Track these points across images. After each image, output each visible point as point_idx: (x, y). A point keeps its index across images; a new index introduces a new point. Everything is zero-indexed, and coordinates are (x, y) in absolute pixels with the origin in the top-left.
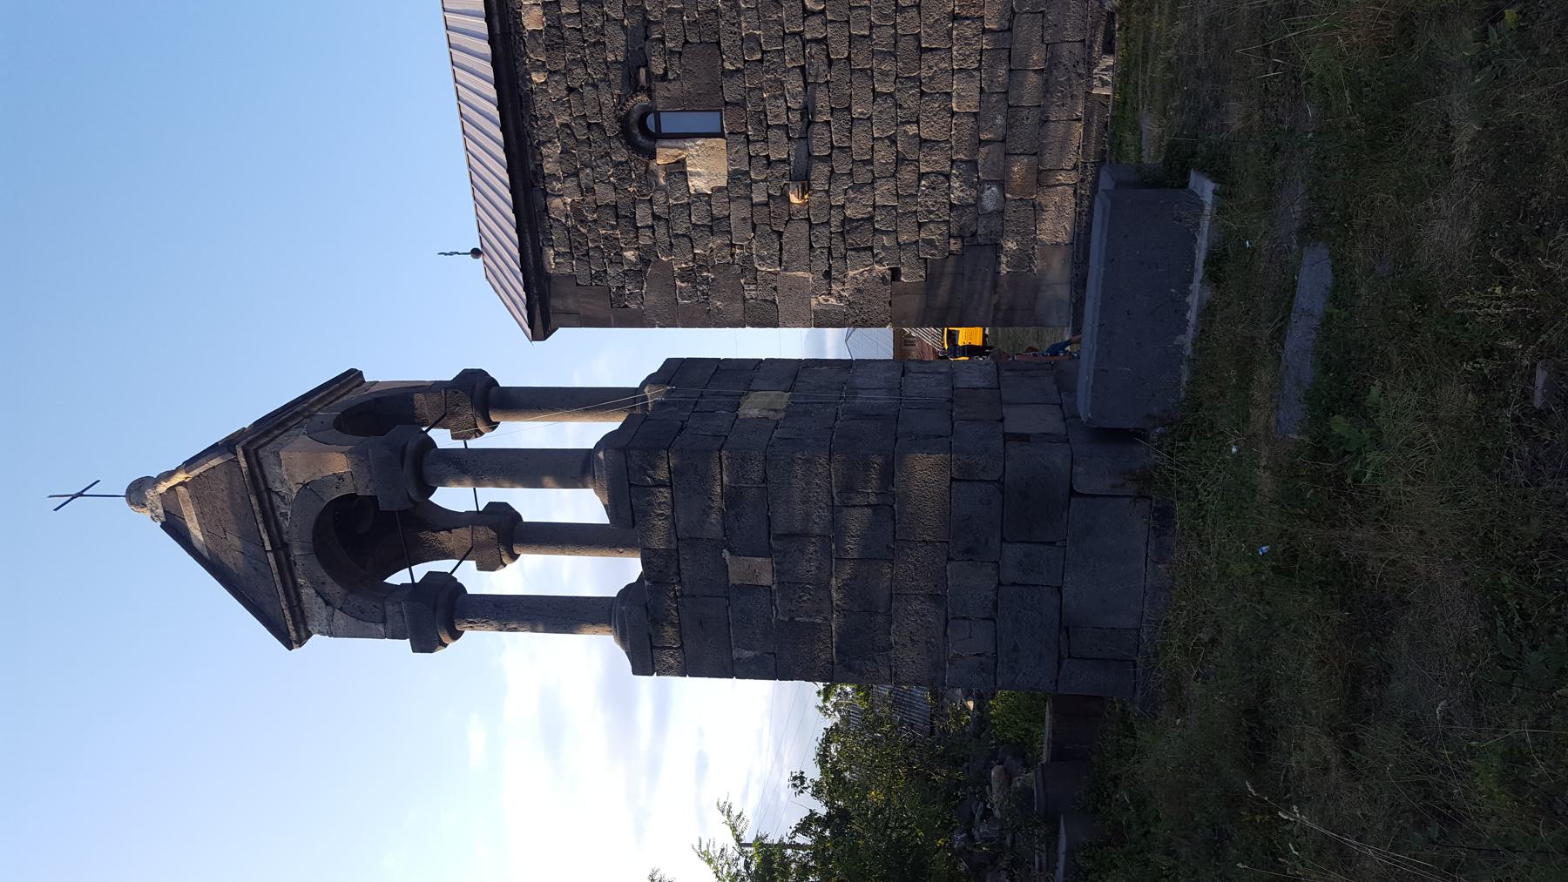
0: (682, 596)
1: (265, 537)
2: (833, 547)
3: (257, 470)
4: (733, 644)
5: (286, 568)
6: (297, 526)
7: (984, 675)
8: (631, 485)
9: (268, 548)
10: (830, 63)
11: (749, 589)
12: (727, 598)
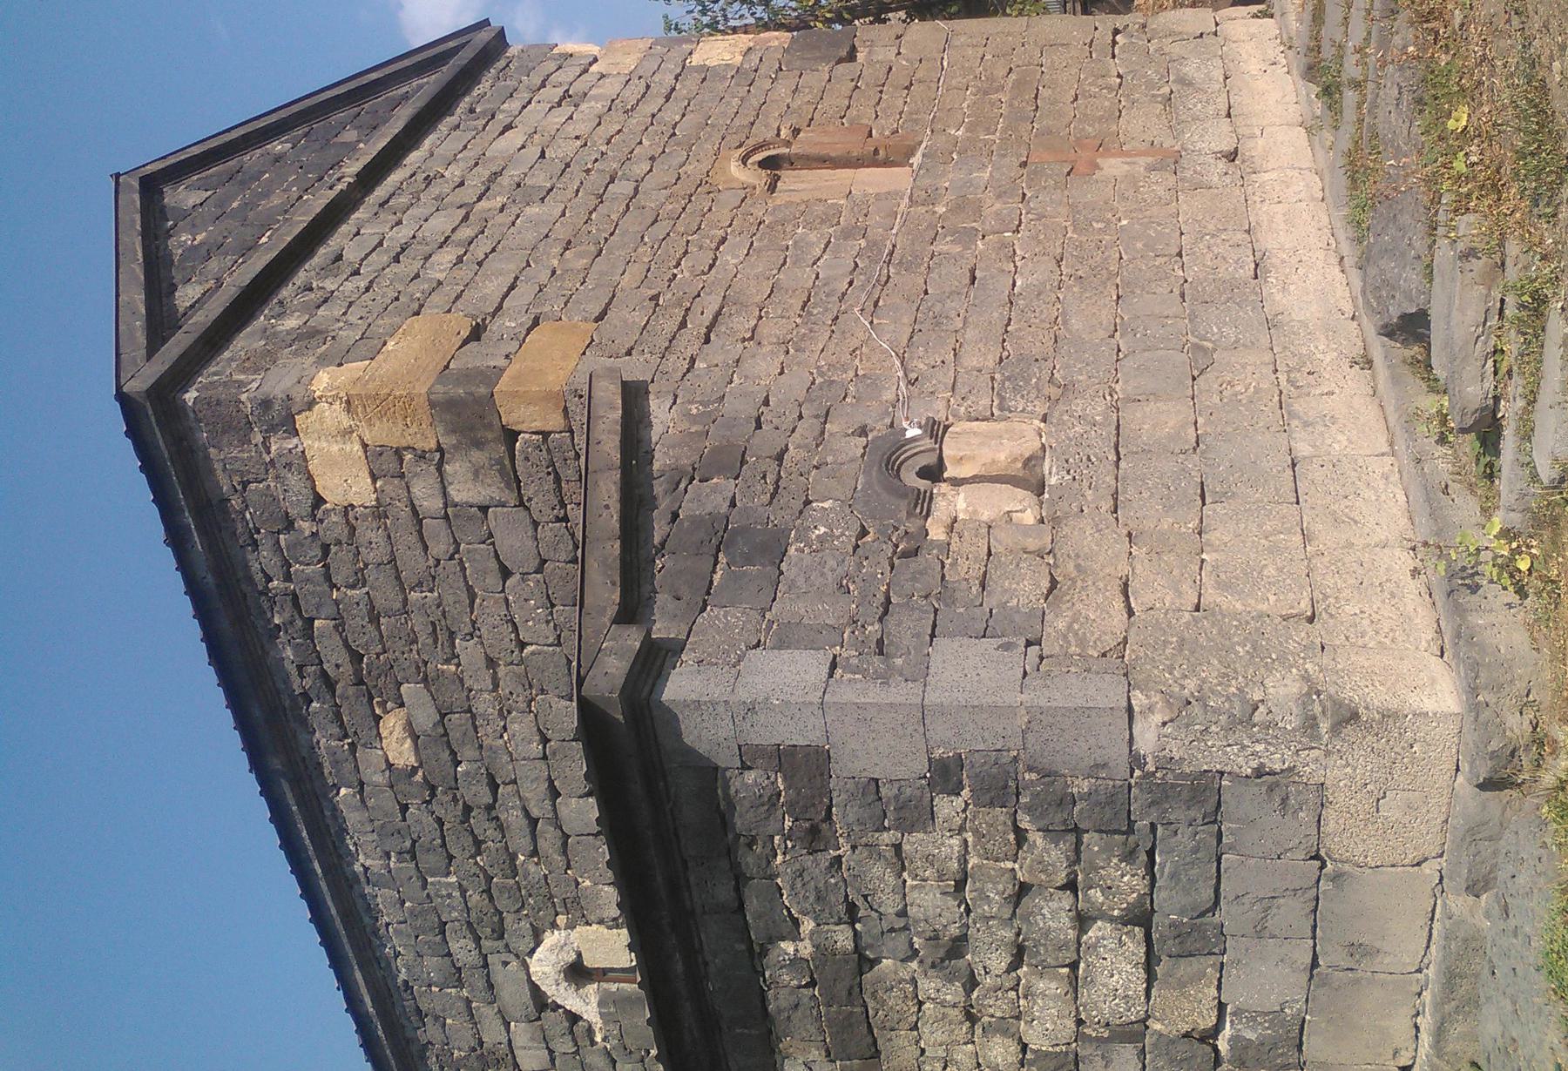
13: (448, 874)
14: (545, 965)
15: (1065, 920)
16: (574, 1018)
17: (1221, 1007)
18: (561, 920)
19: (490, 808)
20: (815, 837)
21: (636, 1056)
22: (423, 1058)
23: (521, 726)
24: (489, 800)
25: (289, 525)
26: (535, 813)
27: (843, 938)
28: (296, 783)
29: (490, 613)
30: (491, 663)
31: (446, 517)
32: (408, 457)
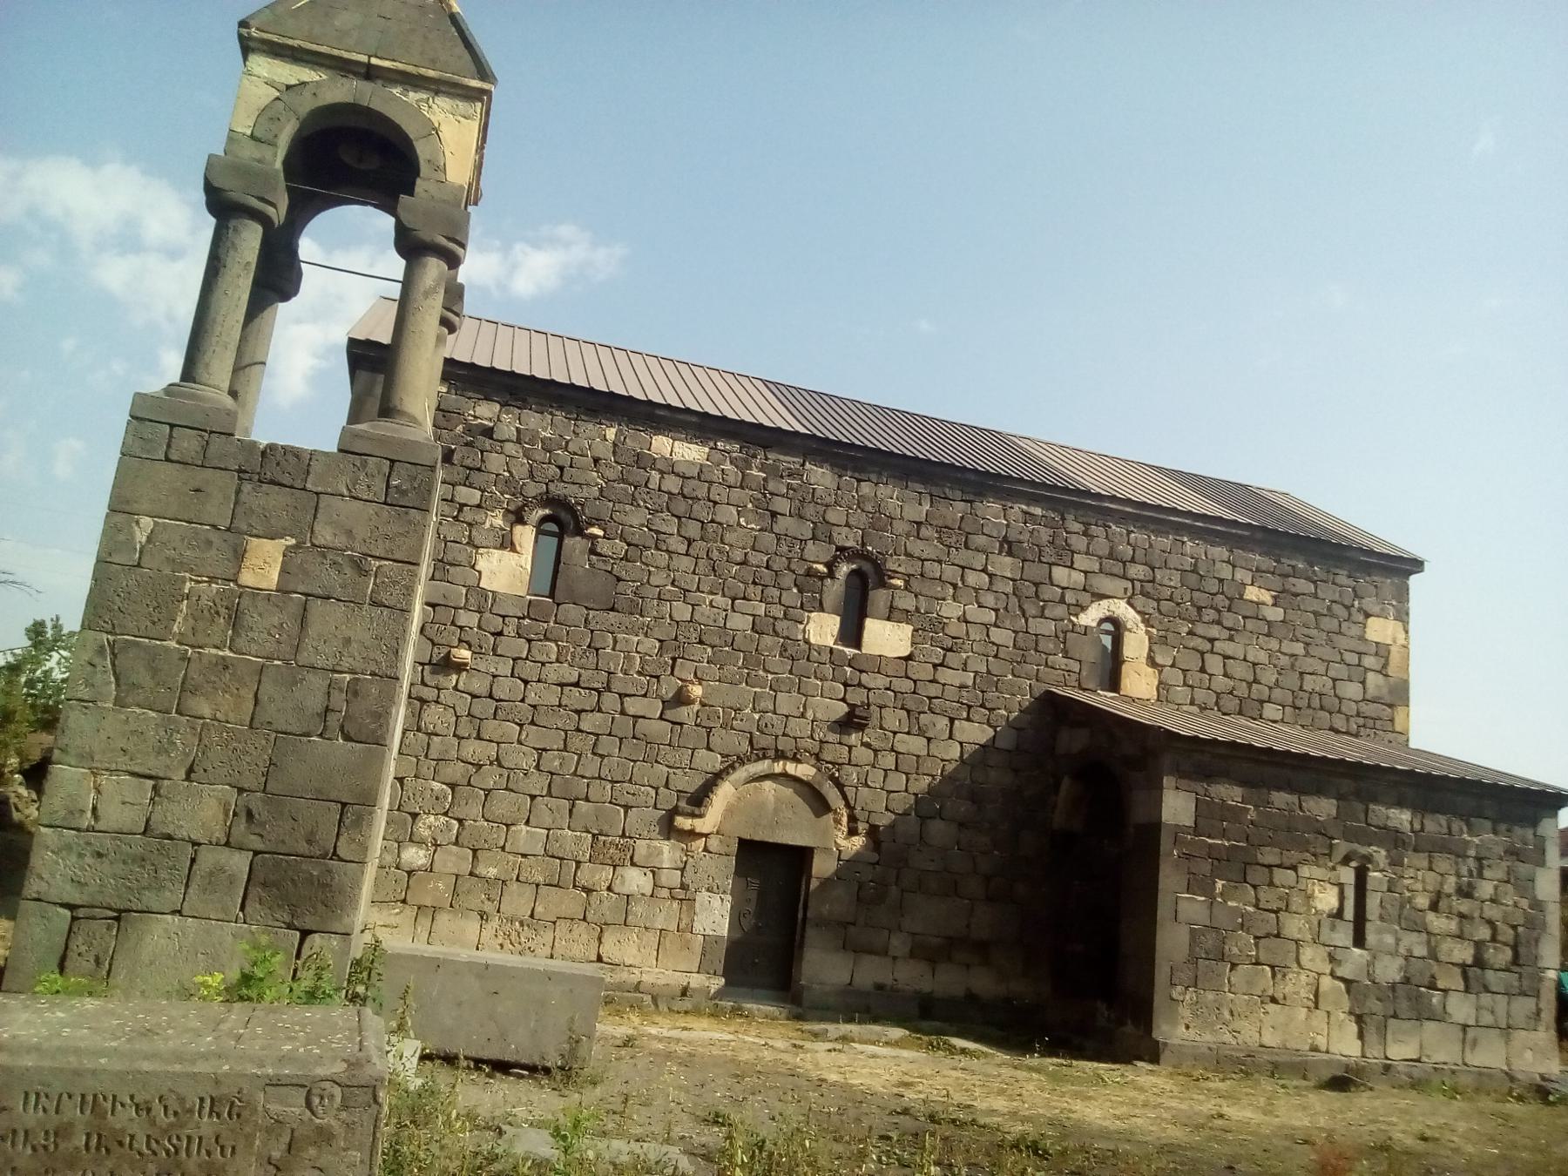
0: (240, 479)
1: (387, 64)
2: (276, 662)
3: (460, 92)
4: (160, 521)
5: (343, 67)
6: (400, 103)
7: (63, 813)
8: (393, 461)
9: (374, 61)
10: (578, 712)
11: (239, 555)
12: (228, 530)
13: (1183, 585)
14: (1122, 609)
15: (1482, 937)
16: (1083, 609)
17: (1445, 991)
18: (1154, 631)
19: (1219, 623)
20: (1514, 853)
21: (1061, 635)
22: (1054, 510)
23: (1262, 657)
24: (1226, 623)
25: (1356, 596)
26: (1217, 644)
27: (1472, 852)
28: (1241, 536)
29: (1321, 668)
30: (1293, 655)
31: (1359, 665)
32: (1383, 660)
